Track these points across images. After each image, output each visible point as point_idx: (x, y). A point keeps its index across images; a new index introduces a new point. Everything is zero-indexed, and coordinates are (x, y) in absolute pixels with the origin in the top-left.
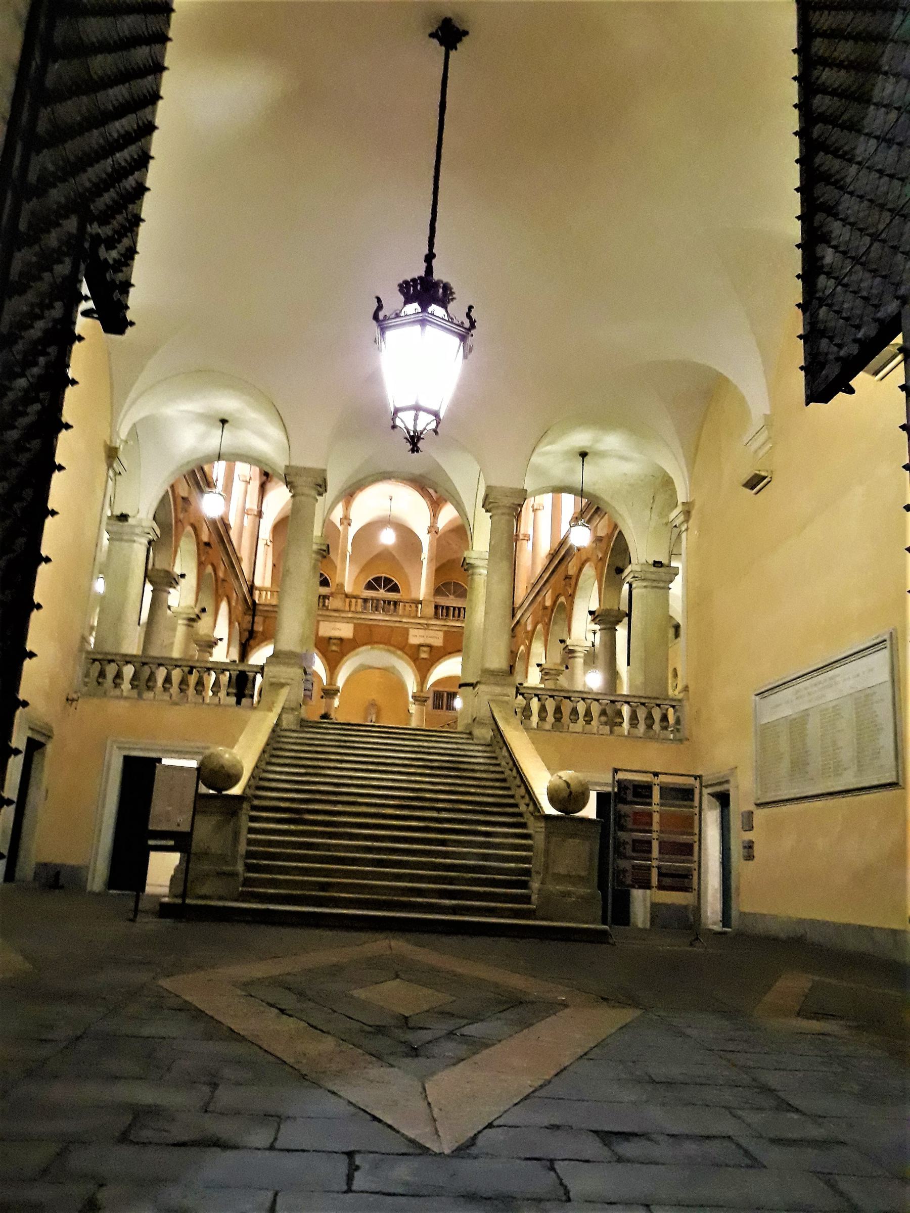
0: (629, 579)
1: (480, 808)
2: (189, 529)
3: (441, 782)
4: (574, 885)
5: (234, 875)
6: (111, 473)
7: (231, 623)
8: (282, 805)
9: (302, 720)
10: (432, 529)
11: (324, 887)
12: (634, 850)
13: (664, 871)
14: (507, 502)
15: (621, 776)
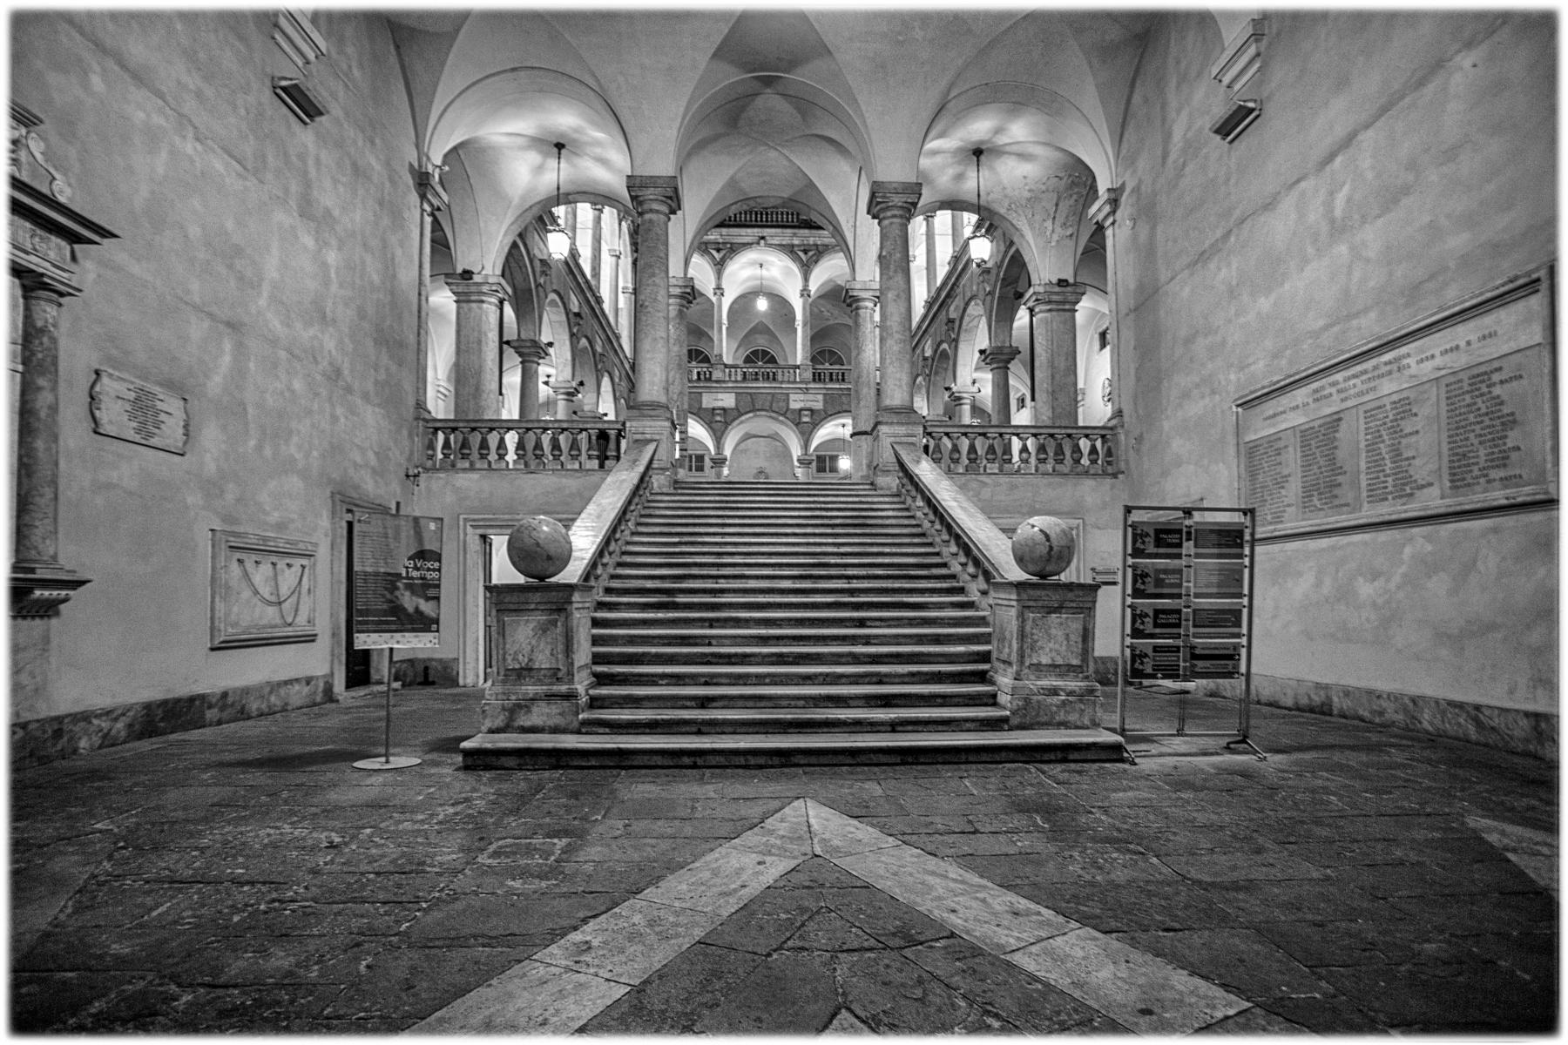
0: (1030, 304)
1: (902, 572)
2: (553, 296)
3: (851, 543)
4: (1061, 676)
5: (570, 696)
6: (427, 207)
7: (615, 398)
8: (649, 584)
9: (676, 482)
10: (805, 293)
11: (704, 702)
12: (1156, 625)
13: (1197, 652)
14: (897, 200)
15: (1136, 516)
